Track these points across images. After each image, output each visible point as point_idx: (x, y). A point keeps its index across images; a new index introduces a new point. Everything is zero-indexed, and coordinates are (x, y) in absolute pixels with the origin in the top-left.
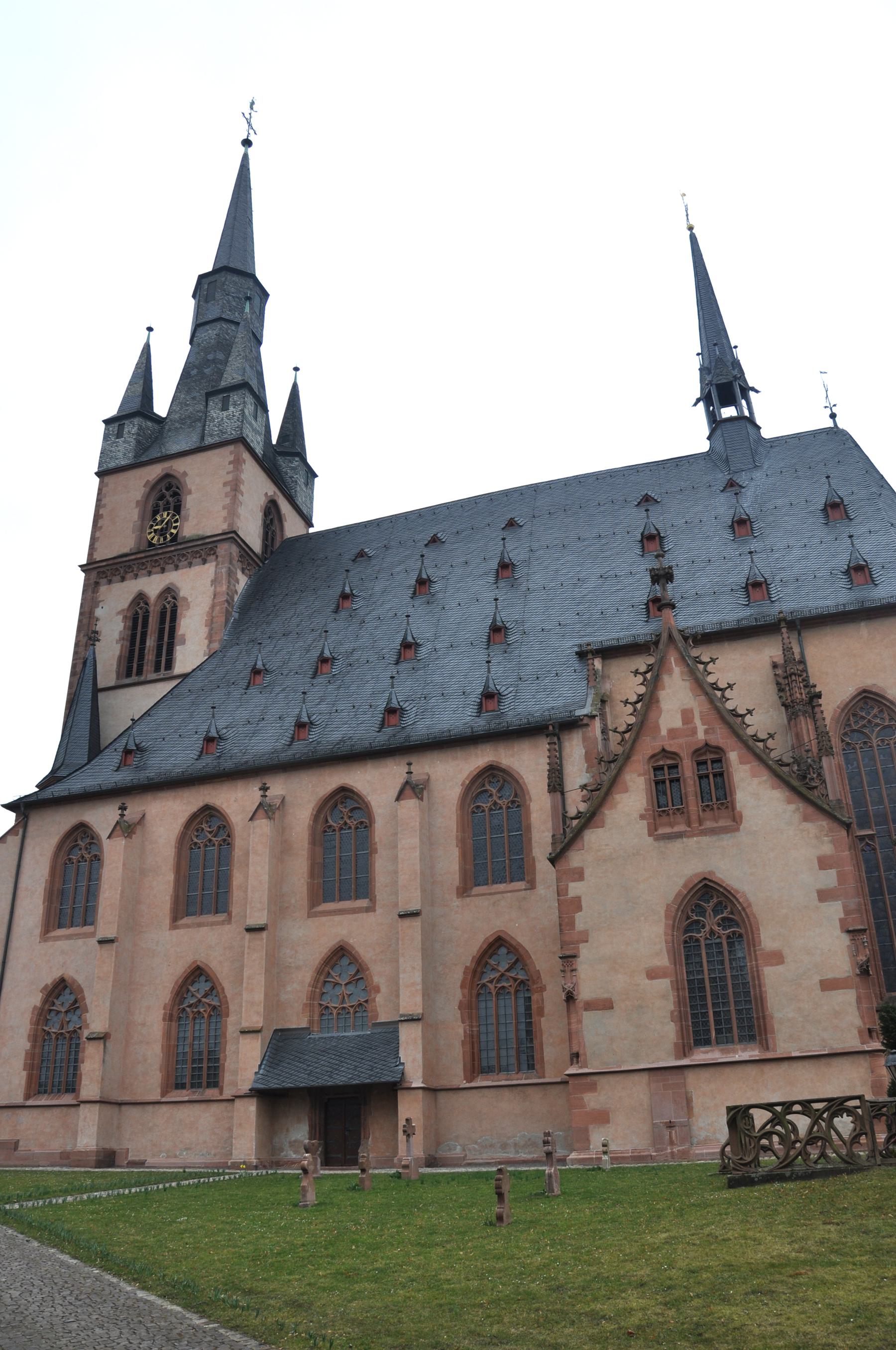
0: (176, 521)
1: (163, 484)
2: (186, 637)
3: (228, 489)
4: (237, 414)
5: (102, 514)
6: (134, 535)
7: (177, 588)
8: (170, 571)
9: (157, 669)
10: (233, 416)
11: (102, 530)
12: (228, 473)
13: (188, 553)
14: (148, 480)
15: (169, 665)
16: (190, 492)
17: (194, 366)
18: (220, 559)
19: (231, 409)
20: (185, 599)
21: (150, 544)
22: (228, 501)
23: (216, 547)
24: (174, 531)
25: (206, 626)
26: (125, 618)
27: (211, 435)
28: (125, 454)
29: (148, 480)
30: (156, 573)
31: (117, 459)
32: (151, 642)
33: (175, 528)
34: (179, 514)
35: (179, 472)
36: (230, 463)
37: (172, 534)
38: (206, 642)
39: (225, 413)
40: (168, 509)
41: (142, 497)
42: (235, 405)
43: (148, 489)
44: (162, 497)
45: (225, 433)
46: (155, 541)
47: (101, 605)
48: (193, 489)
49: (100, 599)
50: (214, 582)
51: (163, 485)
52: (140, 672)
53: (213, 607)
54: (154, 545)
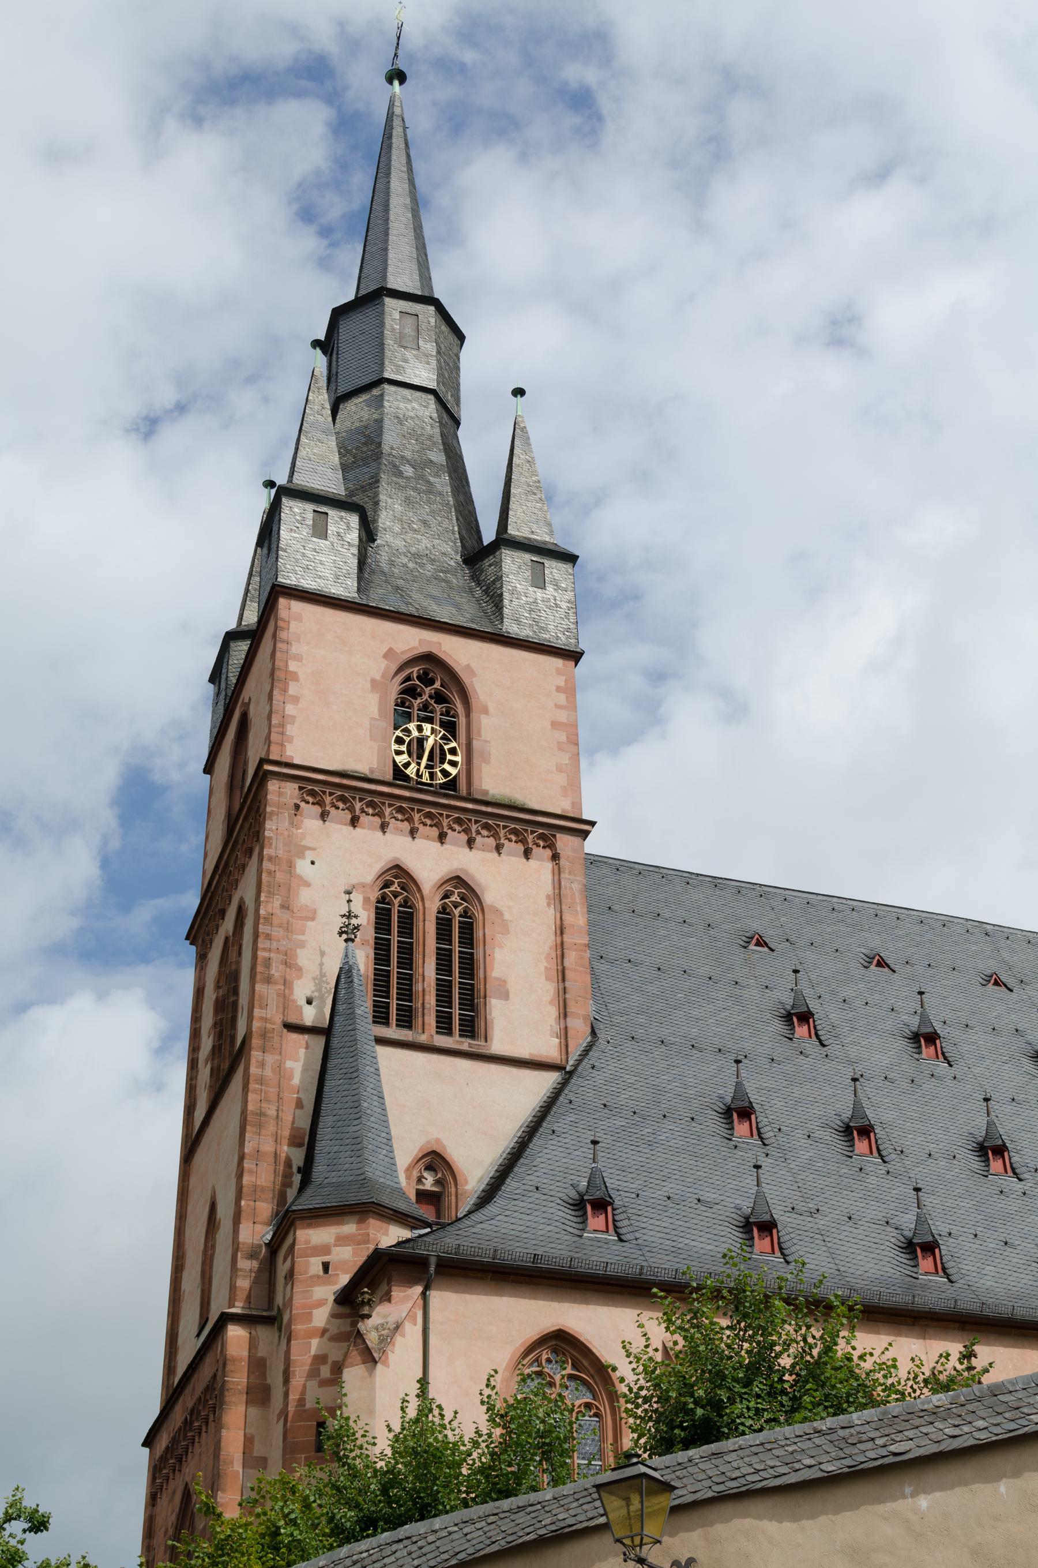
0: (453, 751)
1: (416, 669)
2: (509, 986)
3: (563, 737)
4: (564, 605)
5: (295, 673)
6: (375, 745)
7: (478, 885)
8: (455, 844)
9: (444, 1025)
10: (557, 605)
11: (300, 706)
12: (557, 706)
13: (498, 826)
14: (391, 649)
15: (471, 1027)
16: (485, 711)
17: (403, 457)
18: (563, 862)
19: (550, 589)
20: (497, 911)
21: (399, 773)
22: (565, 759)
23: (554, 836)
24: (453, 771)
25: (547, 979)
26: (366, 900)
27: (518, 621)
28: (337, 577)
29: (391, 649)
30: (427, 838)
31: (320, 577)
32: (428, 970)
33: (454, 764)
34: (455, 740)
35: (459, 664)
36: (559, 689)
37: (445, 773)
38: (553, 1011)
39: (540, 594)
40: (430, 720)
41: (383, 676)
42: (557, 587)
43: (394, 668)
44: (410, 691)
45: (545, 629)
46: (411, 771)
47: (309, 855)
48: (491, 707)
49: (304, 843)
50: (558, 898)
51: (415, 671)
52: (406, 1020)
53: (561, 950)
54: (407, 778)
